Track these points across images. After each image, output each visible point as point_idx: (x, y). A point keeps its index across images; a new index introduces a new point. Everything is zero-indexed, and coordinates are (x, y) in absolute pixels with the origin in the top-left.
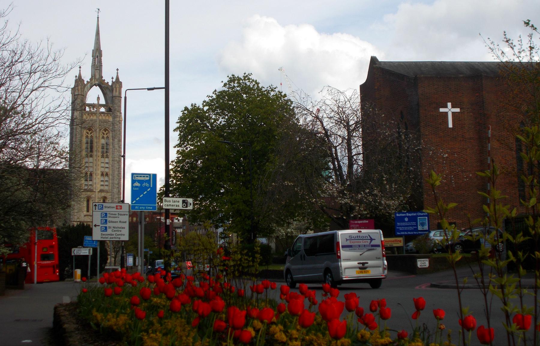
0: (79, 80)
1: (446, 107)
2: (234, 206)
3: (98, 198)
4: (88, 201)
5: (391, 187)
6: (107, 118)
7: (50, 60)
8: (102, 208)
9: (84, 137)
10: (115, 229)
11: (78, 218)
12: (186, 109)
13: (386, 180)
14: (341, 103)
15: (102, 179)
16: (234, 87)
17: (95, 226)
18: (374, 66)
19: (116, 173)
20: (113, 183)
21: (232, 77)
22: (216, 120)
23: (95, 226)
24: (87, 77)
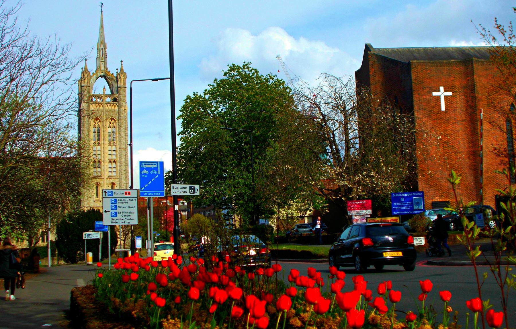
0: (85, 71)
1: (439, 91)
2: (236, 189)
3: (107, 184)
4: (97, 187)
5: (387, 169)
6: (113, 108)
7: (58, 54)
8: (112, 195)
9: (92, 126)
10: (125, 214)
11: (88, 204)
12: (188, 98)
13: (383, 162)
14: (338, 89)
15: (110, 165)
16: (234, 75)
17: (106, 211)
18: (369, 52)
19: (123, 160)
20: (120, 170)
21: (232, 66)
22: (217, 108)
23: (106, 211)
24: (92, 67)
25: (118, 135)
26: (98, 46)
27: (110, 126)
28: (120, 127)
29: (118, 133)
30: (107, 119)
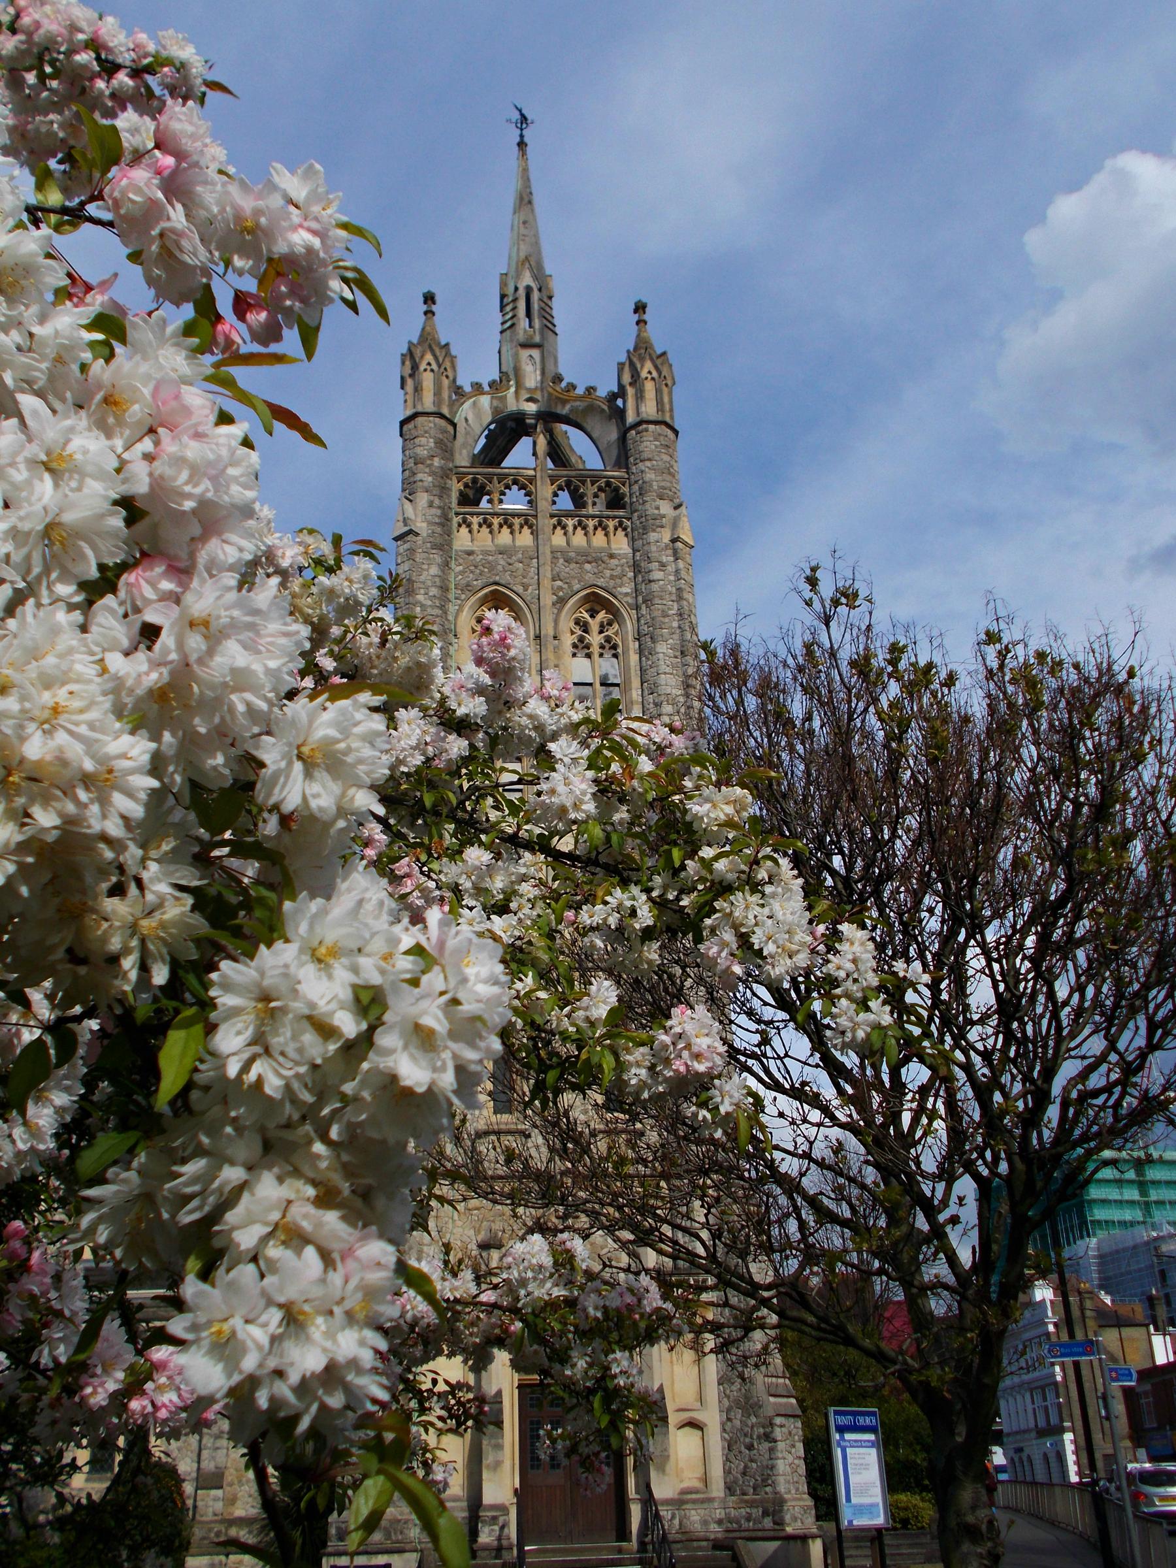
6: (599, 539)
25: (636, 694)
26: (503, 284)
27: (582, 647)
28: (645, 641)
29: (636, 682)
30: (561, 602)
